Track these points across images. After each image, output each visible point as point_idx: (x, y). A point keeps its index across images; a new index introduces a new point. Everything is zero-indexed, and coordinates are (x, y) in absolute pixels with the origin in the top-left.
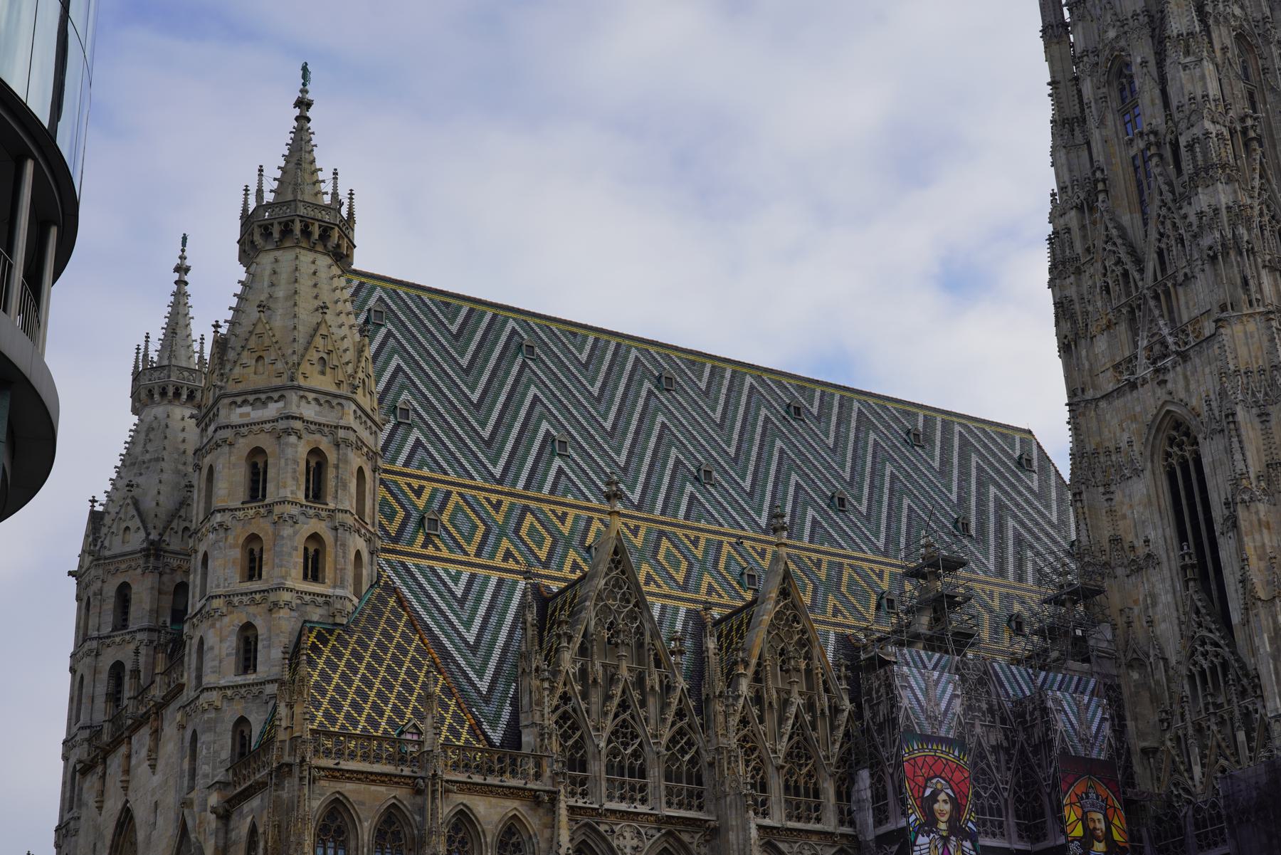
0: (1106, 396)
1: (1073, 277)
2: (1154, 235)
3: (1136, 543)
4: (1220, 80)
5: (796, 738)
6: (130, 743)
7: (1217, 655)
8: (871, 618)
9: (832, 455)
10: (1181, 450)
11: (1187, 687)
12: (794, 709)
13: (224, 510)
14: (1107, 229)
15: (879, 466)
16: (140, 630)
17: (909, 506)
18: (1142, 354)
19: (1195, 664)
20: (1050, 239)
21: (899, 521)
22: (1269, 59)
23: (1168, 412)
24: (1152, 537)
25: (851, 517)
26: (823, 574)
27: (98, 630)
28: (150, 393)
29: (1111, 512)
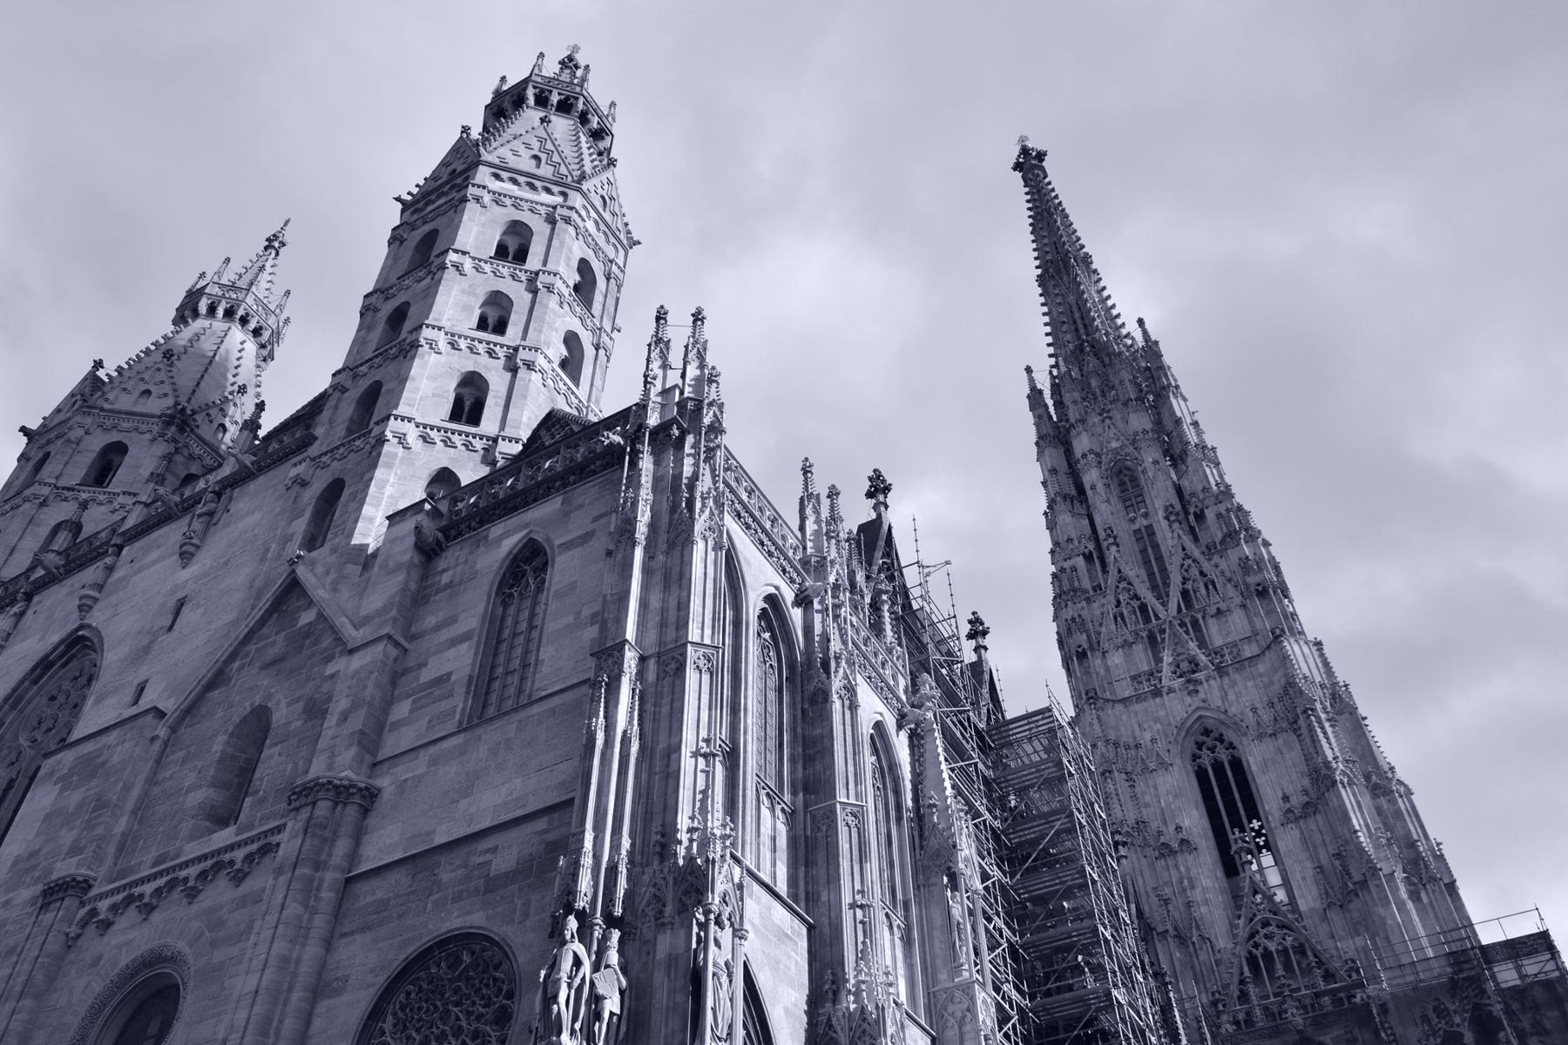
0: (1124, 701)
1: (1084, 603)
3: (1163, 828)
6: (118, 555)
10: (1213, 752)
11: (1246, 969)
13: (464, 253)
14: (1119, 571)
16: (124, 493)
19: (1256, 946)
20: (1054, 576)
23: (1200, 717)
24: (1186, 823)
27: (57, 478)
28: (212, 310)
29: (1134, 797)
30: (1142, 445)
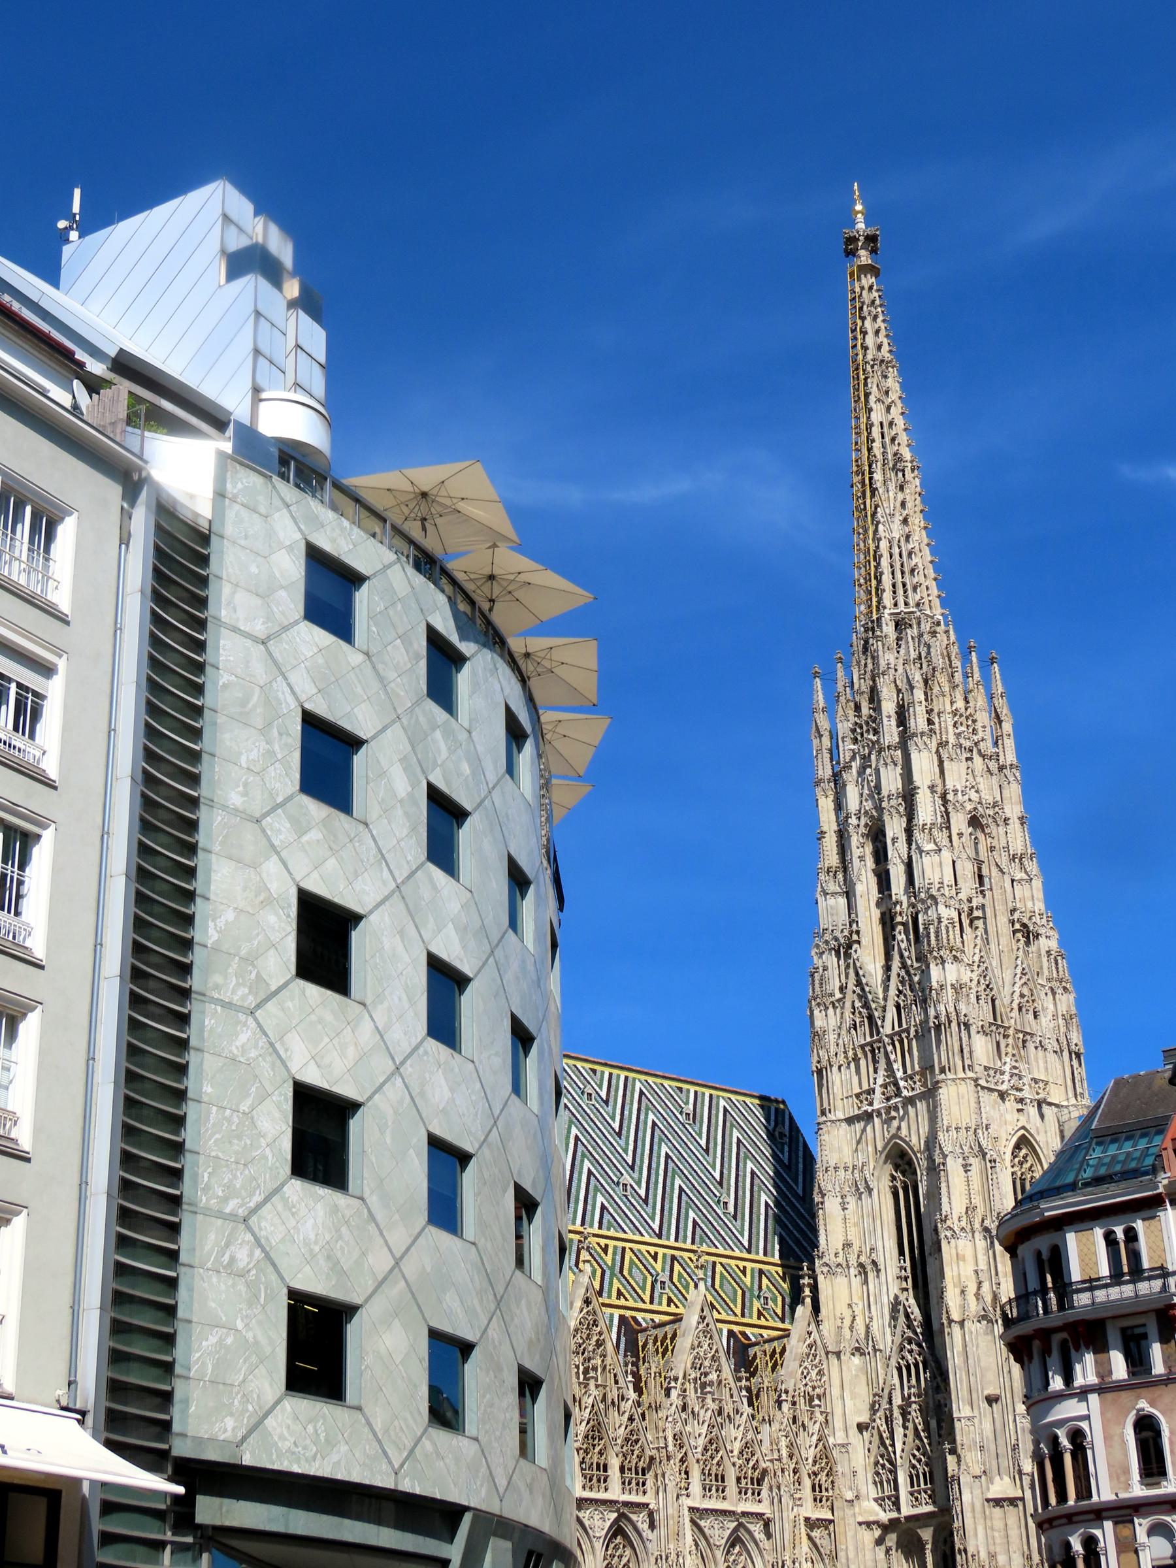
0: (850, 1121)
2: (893, 992)
4: (954, 862)
5: (592, 1423)
7: (919, 1355)
8: (647, 1299)
9: (618, 1139)
12: (590, 1401)
14: (857, 974)
15: (656, 1147)
17: (680, 1187)
18: (878, 1090)
19: (903, 1358)
21: (671, 1202)
22: (996, 838)
23: (895, 1143)
25: (633, 1201)
26: (609, 1259)
30: (886, 818)
